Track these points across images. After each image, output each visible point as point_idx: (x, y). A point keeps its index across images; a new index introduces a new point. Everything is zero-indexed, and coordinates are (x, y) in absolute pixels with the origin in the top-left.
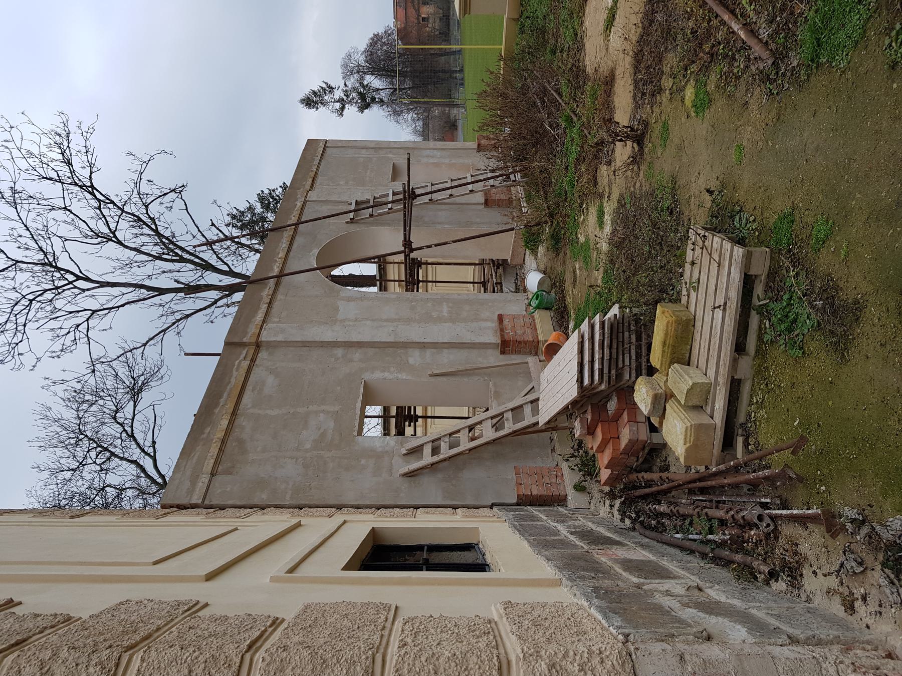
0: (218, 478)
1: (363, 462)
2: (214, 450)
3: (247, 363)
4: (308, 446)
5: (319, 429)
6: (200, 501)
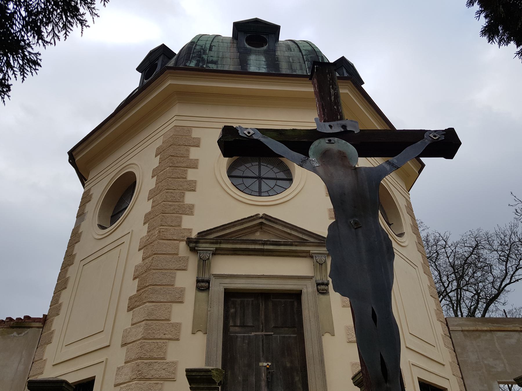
0: (461, 333)
1: (485, 385)
4: (486, 362)
5: (495, 365)
6: (451, 330)
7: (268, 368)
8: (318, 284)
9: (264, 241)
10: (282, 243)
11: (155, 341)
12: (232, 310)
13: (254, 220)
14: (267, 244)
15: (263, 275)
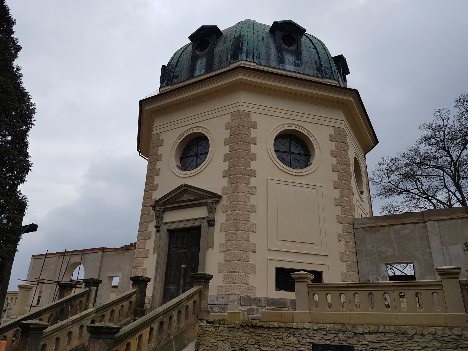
4: (379, 250)
7: (184, 268)
8: (208, 221)
9: (183, 200)
10: (192, 200)
11: (139, 259)
12: (173, 240)
14: (185, 202)
15: (183, 220)
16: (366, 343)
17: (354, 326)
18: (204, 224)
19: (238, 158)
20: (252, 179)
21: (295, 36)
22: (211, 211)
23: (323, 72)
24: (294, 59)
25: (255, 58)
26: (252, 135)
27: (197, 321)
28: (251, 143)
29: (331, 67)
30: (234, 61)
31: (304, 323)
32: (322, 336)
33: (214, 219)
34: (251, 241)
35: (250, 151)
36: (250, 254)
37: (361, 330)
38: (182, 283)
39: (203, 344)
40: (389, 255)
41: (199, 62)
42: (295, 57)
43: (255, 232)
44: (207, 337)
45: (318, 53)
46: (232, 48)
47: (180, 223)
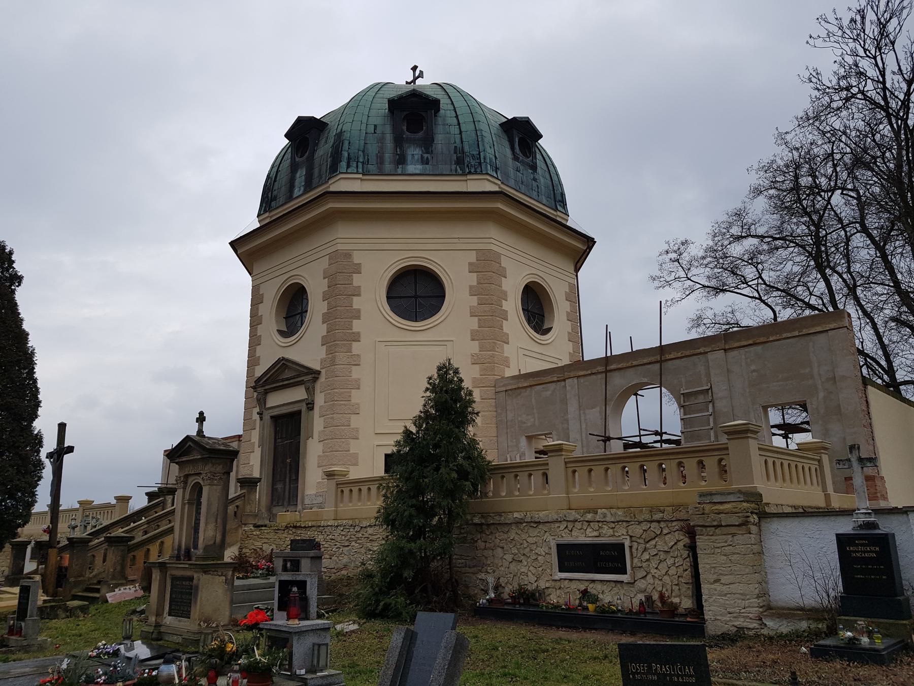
2: (514, 387)
3: (555, 379)
4: (519, 419)
13: (279, 363)
16: (367, 536)
17: (360, 520)
18: (304, 408)
19: (336, 319)
20: (355, 344)
21: (422, 113)
22: (310, 391)
23: (466, 165)
24: (420, 153)
25: (360, 165)
26: (355, 284)
27: (239, 526)
28: (354, 295)
29: (479, 154)
30: (333, 173)
31: (328, 520)
32: (340, 532)
33: (313, 401)
34: (353, 425)
35: (352, 307)
36: (352, 442)
37: (365, 524)
38: (287, 480)
39: (246, 548)
40: (529, 425)
41: (298, 175)
42: (423, 148)
43: (358, 414)
44: (251, 541)
45: (461, 133)
46: (331, 153)
47: (282, 408)
